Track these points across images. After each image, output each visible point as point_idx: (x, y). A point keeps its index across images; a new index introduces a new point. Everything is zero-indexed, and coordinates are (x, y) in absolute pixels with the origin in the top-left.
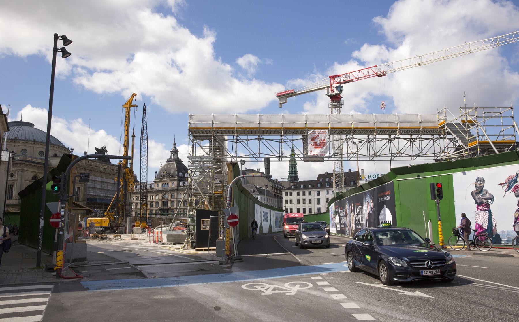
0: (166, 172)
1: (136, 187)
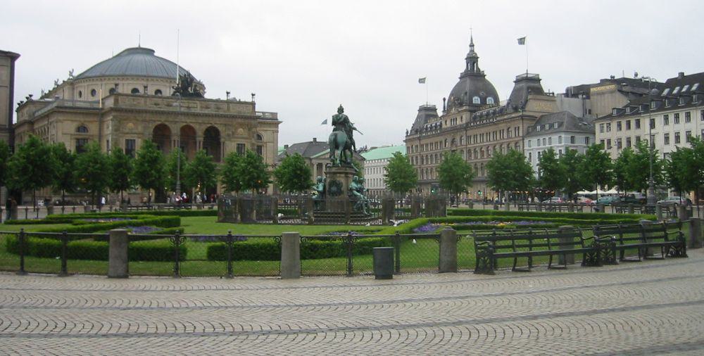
1: (427, 129)
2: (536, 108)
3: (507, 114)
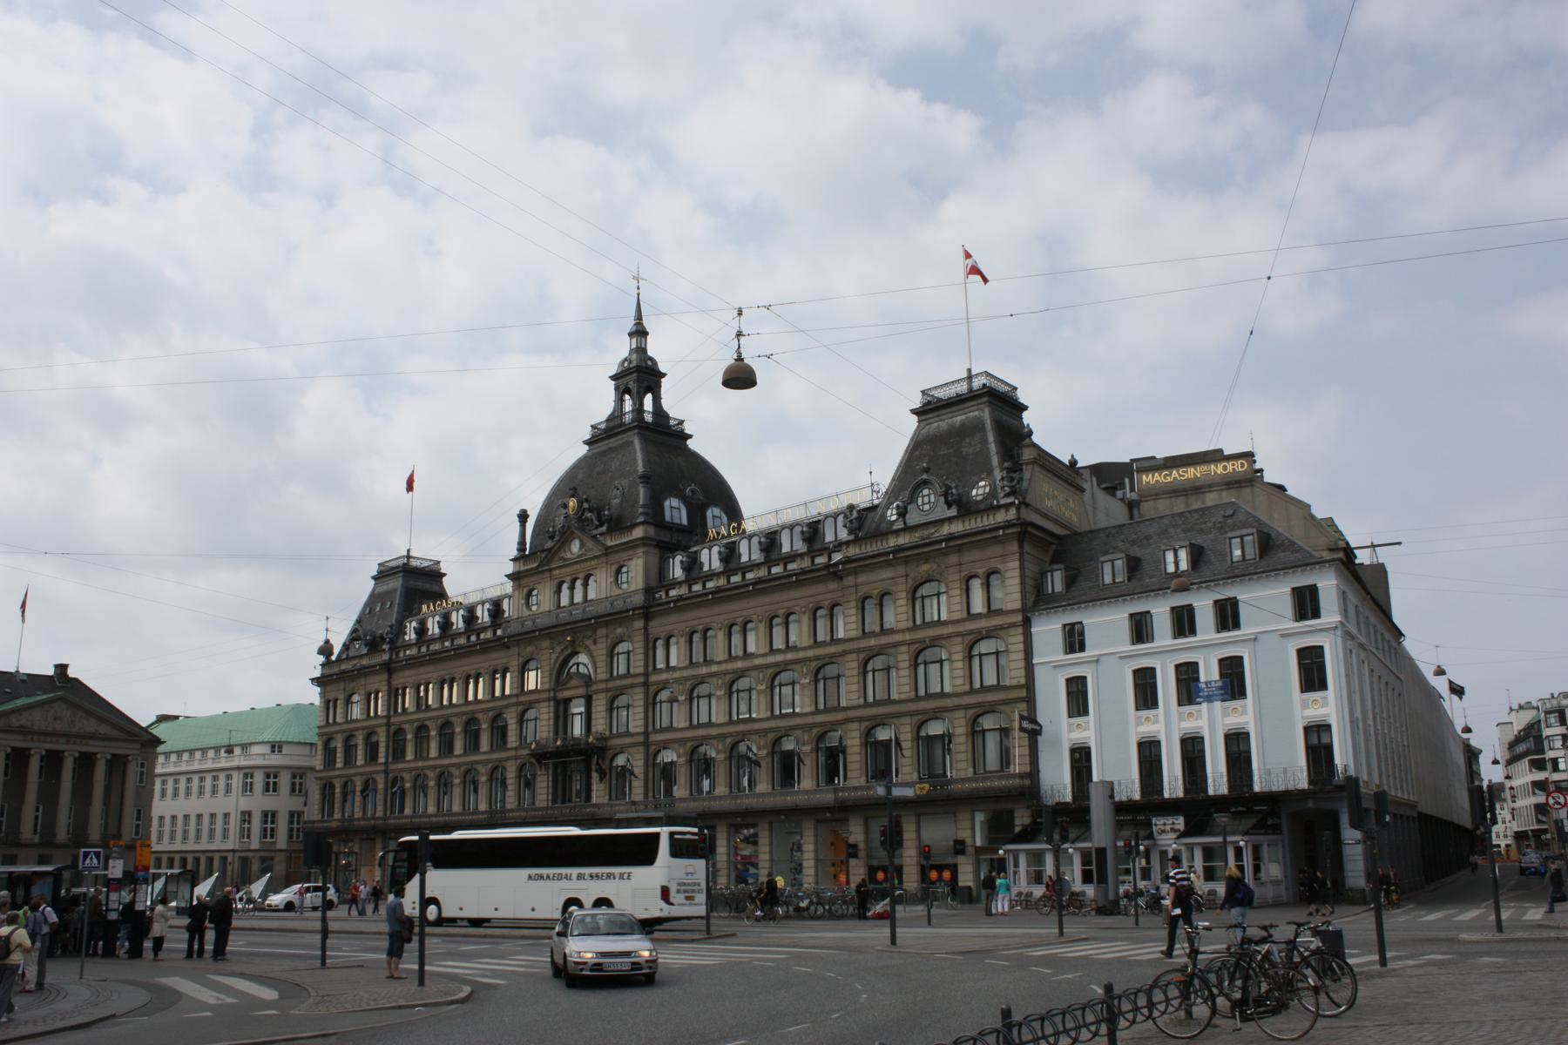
0: (580, 503)
1: (422, 630)
2: (1049, 503)
3: (908, 529)
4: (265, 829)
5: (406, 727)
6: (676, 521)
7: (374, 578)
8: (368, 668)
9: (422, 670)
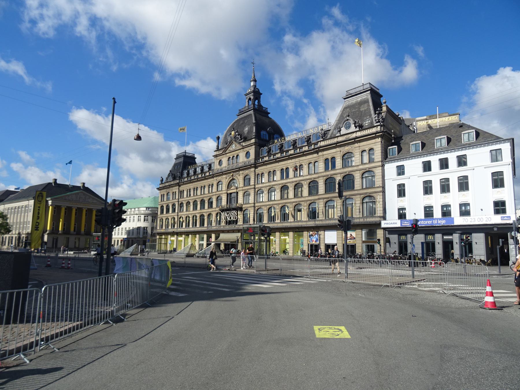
1: (188, 174)
4: (144, 232)
5: (183, 202)
6: (265, 138)
7: (175, 159)
8: (173, 185)
9: (188, 185)
